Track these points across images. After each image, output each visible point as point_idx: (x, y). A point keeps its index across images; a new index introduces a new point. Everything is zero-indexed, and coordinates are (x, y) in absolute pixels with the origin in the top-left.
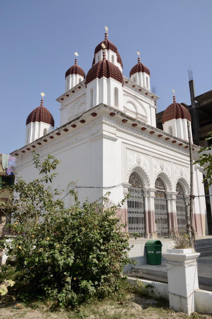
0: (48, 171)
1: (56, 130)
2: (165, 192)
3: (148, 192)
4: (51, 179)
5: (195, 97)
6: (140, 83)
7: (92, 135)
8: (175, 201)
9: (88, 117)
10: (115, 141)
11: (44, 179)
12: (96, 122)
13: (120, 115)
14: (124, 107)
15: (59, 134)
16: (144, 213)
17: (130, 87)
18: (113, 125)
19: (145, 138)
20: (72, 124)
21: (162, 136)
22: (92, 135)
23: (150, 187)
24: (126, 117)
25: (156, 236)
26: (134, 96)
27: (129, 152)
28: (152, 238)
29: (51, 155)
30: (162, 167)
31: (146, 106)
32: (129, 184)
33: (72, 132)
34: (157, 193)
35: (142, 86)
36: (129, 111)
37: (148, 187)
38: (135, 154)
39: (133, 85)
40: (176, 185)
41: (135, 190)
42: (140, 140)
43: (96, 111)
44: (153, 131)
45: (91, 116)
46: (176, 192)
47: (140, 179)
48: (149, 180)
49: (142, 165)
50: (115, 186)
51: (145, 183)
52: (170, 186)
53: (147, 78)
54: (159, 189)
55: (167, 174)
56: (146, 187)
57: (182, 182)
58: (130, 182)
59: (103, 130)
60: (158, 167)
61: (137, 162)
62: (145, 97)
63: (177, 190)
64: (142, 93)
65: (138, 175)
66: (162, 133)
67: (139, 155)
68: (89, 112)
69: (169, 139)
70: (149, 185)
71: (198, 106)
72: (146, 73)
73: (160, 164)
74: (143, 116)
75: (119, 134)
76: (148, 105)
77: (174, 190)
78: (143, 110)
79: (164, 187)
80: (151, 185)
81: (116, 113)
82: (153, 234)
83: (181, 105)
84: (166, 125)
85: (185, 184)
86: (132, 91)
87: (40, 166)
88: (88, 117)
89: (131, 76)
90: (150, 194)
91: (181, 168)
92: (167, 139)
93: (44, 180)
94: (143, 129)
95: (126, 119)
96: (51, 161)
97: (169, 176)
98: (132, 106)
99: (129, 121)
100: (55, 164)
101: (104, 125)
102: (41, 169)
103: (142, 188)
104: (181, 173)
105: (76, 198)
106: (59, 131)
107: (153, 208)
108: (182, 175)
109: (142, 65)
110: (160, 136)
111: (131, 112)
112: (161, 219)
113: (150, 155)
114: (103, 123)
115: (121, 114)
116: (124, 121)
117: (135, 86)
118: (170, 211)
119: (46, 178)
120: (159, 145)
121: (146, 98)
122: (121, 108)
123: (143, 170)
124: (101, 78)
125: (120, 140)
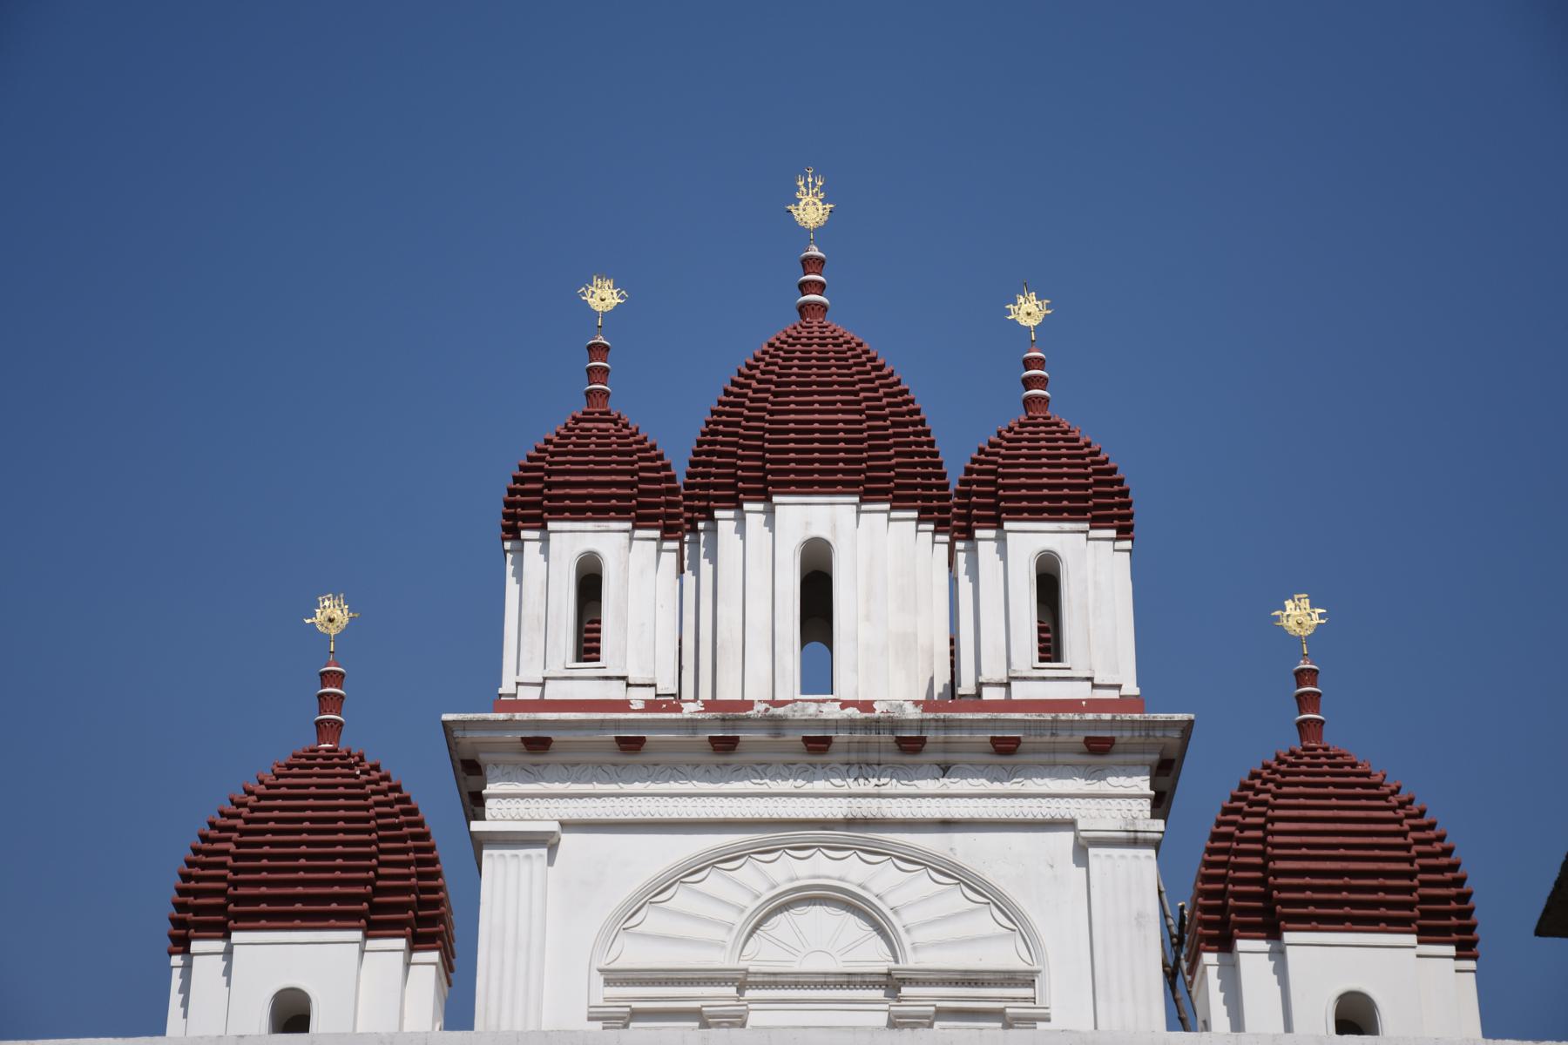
17: (788, 764)
26: (850, 823)
62: (992, 779)
64: (940, 758)
111: (825, 985)
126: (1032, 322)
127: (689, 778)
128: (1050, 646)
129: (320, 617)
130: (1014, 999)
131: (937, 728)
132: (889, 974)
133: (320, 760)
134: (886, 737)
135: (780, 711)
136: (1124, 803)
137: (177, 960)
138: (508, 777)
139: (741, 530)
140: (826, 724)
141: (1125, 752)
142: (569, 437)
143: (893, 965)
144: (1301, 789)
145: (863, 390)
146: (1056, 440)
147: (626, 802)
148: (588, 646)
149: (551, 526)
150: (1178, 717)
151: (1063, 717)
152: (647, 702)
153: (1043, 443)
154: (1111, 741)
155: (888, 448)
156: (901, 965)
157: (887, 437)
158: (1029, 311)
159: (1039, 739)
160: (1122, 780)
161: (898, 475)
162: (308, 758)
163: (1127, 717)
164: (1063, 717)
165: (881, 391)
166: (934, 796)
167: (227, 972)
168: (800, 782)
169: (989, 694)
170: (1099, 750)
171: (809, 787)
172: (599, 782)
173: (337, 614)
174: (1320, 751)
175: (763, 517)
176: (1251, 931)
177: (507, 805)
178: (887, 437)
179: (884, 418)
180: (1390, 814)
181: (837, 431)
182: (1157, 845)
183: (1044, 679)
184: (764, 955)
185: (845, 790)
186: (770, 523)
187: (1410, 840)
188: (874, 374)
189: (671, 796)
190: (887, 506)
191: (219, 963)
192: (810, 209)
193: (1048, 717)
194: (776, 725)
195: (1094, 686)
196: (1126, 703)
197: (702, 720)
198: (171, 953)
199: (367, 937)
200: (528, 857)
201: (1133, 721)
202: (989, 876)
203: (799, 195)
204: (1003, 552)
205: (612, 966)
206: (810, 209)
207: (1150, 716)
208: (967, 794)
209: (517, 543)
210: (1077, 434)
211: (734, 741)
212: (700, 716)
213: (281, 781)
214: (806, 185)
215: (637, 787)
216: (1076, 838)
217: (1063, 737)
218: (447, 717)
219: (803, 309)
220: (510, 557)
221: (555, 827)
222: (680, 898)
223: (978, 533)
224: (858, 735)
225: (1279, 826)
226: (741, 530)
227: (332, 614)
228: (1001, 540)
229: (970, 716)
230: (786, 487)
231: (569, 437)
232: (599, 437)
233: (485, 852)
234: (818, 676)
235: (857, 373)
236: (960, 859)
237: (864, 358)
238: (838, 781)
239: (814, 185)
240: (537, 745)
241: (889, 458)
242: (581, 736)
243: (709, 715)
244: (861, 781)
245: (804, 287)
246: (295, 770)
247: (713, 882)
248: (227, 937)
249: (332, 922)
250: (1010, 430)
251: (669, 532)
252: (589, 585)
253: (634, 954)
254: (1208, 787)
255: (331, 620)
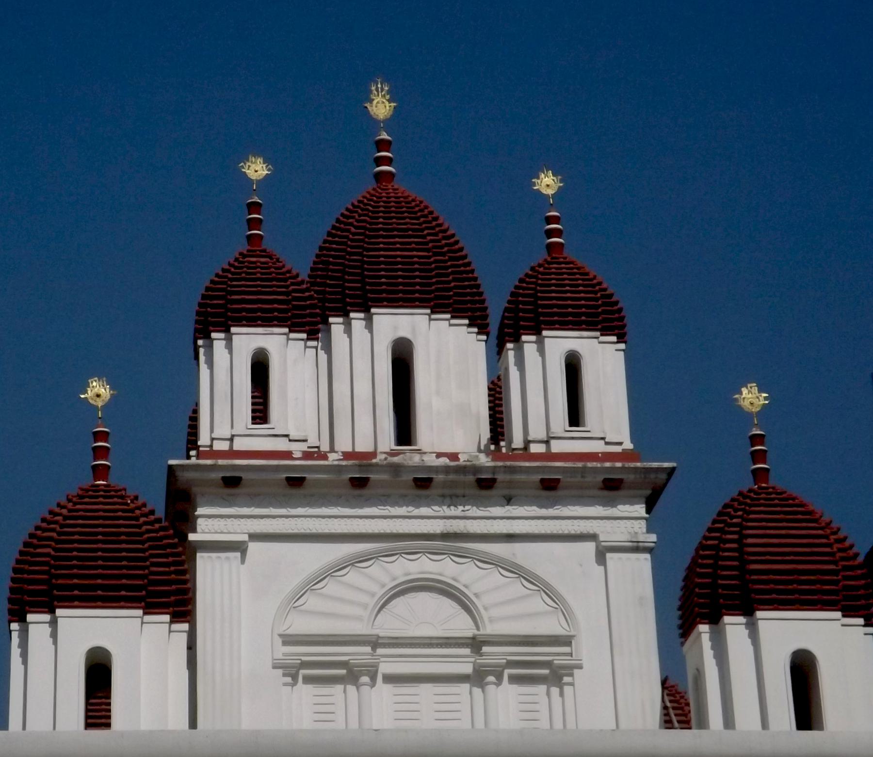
26: (445, 536)
62: (541, 506)
64: (506, 492)
83: (716, 525)
98: (448, 606)
111: (430, 645)
121: (551, 512)
126: (550, 192)
127: (336, 505)
128: (575, 416)
129: (90, 394)
130: (558, 654)
131: (505, 472)
132: (474, 638)
133: (102, 493)
134: (471, 478)
135: (396, 459)
136: (629, 523)
137: (15, 626)
138: (211, 504)
139: (348, 331)
140: (430, 469)
141: (630, 488)
142: (241, 268)
143: (476, 632)
144: (762, 516)
145: (429, 234)
146: (575, 274)
147: (292, 521)
148: (261, 414)
149: (233, 330)
150: (666, 465)
151: (589, 465)
152: (304, 453)
153: (565, 276)
154: (621, 481)
155: (448, 275)
156: (482, 632)
157: (447, 268)
158: (547, 183)
159: (573, 480)
160: (627, 507)
161: (456, 294)
162: (94, 491)
163: (632, 465)
164: (589, 465)
165: (441, 235)
167: (54, 635)
168: (411, 508)
169: (535, 448)
170: (612, 487)
172: (274, 507)
173: (102, 391)
174: (771, 490)
175: (364, 323)
176: (734, 611)
177: (211, 523)
178: (447, 268)
179: (443, 254)
180: (820, 532)
181: (414, 263)
182: (650, 550)
183: (573, 438)
184: (389, 624)
185: (441, 514)
186: (369, 326)
187: (835, 550)
188: (434, 223)
189: (323, 517)
190: (448, 316)
191: (47, 629)
192: (381, 106)
193: (580, 465)
194: (396, 469)
195: (607, 443)
196: (625, 456)
197: (346, 466)
198: (10, 622)
199: (145, 613)
200: (228, 558)
201: (636, 468)
202: (539, 572)
203: (372, 97)
204: (541, 351)
205: (289, 632)
206: (381, 106)
208: (523, 517)
209: (207, 341)
210: (587, 270)
211: (367, 480)
212: (344, 463)
213: (78, 507)
214: (377, 90)
215: (300, 511)
216: (597, 547)
217: (589, 479)
218: (172, 462)
219: (379, 176)
220: (202, 351)
221: (245, 538)
222: (331, 587)
223: (524, 338)
224: (451, 477)
225: (750, 541)
226: (348, 331)
227: (98, 391)
228: (540, 344)
229: (527, 464)
230: (381, 303)
231: (241, 268)
232: (262, 268)
233: (198, 555)
234: (405, 432)
235: (418, 220)
236: (519, 561)
237: (426, 212)
238: (436, 508)
239: (382, 90)
240: (232, 482)
241: (449, 282)
242: (264, 476)
243: (350, 462)
244: (452, 508)
245: (379, 161)
246: (87, 500)
247: (352, 576)
248: (52, 611)
249: (122, 604)
250: (540, 265)
251: (312, 335)
252: (260, 369)
253: (301, 625)
254: (696, 511)
255: (98, 396)
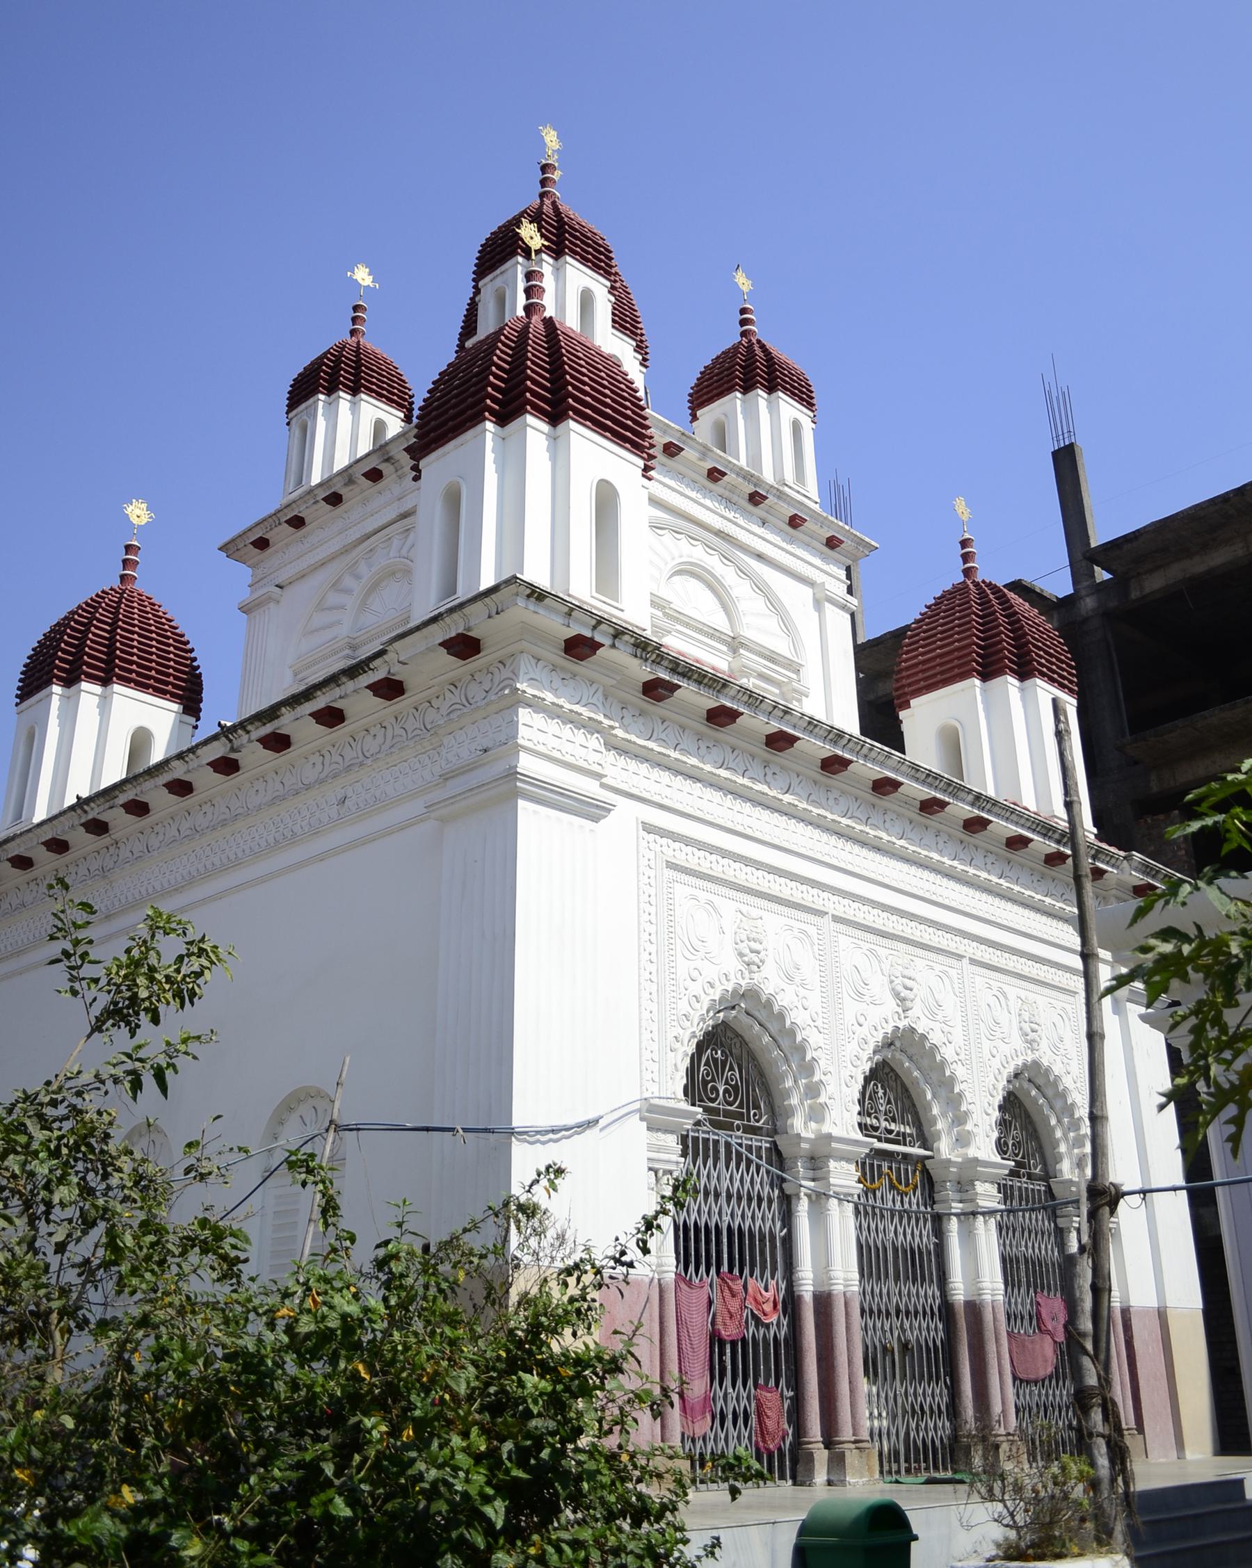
0: (144, 1018)
1: (215, 738)
2: (927, 1162)
3: (816, 1163)
4: (169, 1073)
5: (1093, 545)
6: (755, 458)
7: (446, 777)
8: (992, 1223)
9: (425, 665)
10: (596, 819)
11: (119, 1072)
12: (475, 691)
13: (630, 649)
14: (657, 602)
15: (227, 766)
16: (791, 1304)
18: (586, 712)
19: (788, 798)
20: (320, 702)
21: (896, 785)
22: (446, 777)
23: (827, 1128)
24: (665, 663)
25: (871, 1474)
26: (719, 533)
27: (684, 889)
28: (843, 1482)
29: (165, 908)
30: (904, 993)
31: (796, 597)
32: (684, 1106)
33: (317, 759)
34: (870, 1168)
35: (768, 476)
36: (687, 625)
37: (813, 1125)
38: (729, 904)
39: (709, 465)
40: (996, 1114)
41: (728, 1145)
42: (758, 812)
43: (477, 623)
44: (840, 753)
45: (446, 659)
46: (997, 1159)
47: (762, 1074)
48: (816, 1079)
49: (771, 983)
50: (591, 1124)
51: (794, 1101)
52: (960, 1119)
53: (796, 427)
54: (888, 1141)
55: (935, 1038)
56: (799, 1125)
57: (1033, 1093)
58: (694, 1090)
59: (517, 748)
60: (879, 988)
61: (741, 955)
63: (1001, 1147)
64: (764, 514)
65: (744, 1043)
66: (896, 770)
67: (755, 913)
68: (433, 628)
69: (943, 805)
70: (817, 1114)
71: (1113, 604)
72: (793, 395)
73: (886, 966)
74: (772, 657)
75: (622, 771)
76: (808, 592)
77: (984, 1147)
78: (773, 623)
79: (918, 1124)
80: (831, 1110)
81: (607, 641)
82: (852, 1458)
83: (1011, 595)
84: (923, 718)
85: (1058, 1104)
86: (708, 502)
87: (96, 981)
88: (425, 665)
89: (699, 413)
90: (825, 1178)
91: (1023, 994)
92: (930, 807)
93: (116, 1081)
94: (779, 741)
95: (665, 676)
96: (169, 948)
97: (948, 1053)
99: (688, 692)
100: (196, 968)
101: (524, 715)
102: (104, 1000)
103: (775, 1131)
104: (1027, 1028)
105: (329, 1208)
106: (233, 750)
107: (845, 1274)
108: (1031, 1044)
109: (763, 347)
110: (884, 787)
111: (700, 631)
112: (905, 1347)
113: (821, 914)
114: (519, 700)
115: (636, 645)
116: (655, 690)
117: (724, 474)
118: (959, 1292)
119: (130, 1065)
120: (878, 848)
121: (789, 547)
122: (634, 611)
123: (776, 1008)
124: (514, 426)
125: (626, 813)
166: (760, 537)
171: (702, 501)
207: (863, 537)
